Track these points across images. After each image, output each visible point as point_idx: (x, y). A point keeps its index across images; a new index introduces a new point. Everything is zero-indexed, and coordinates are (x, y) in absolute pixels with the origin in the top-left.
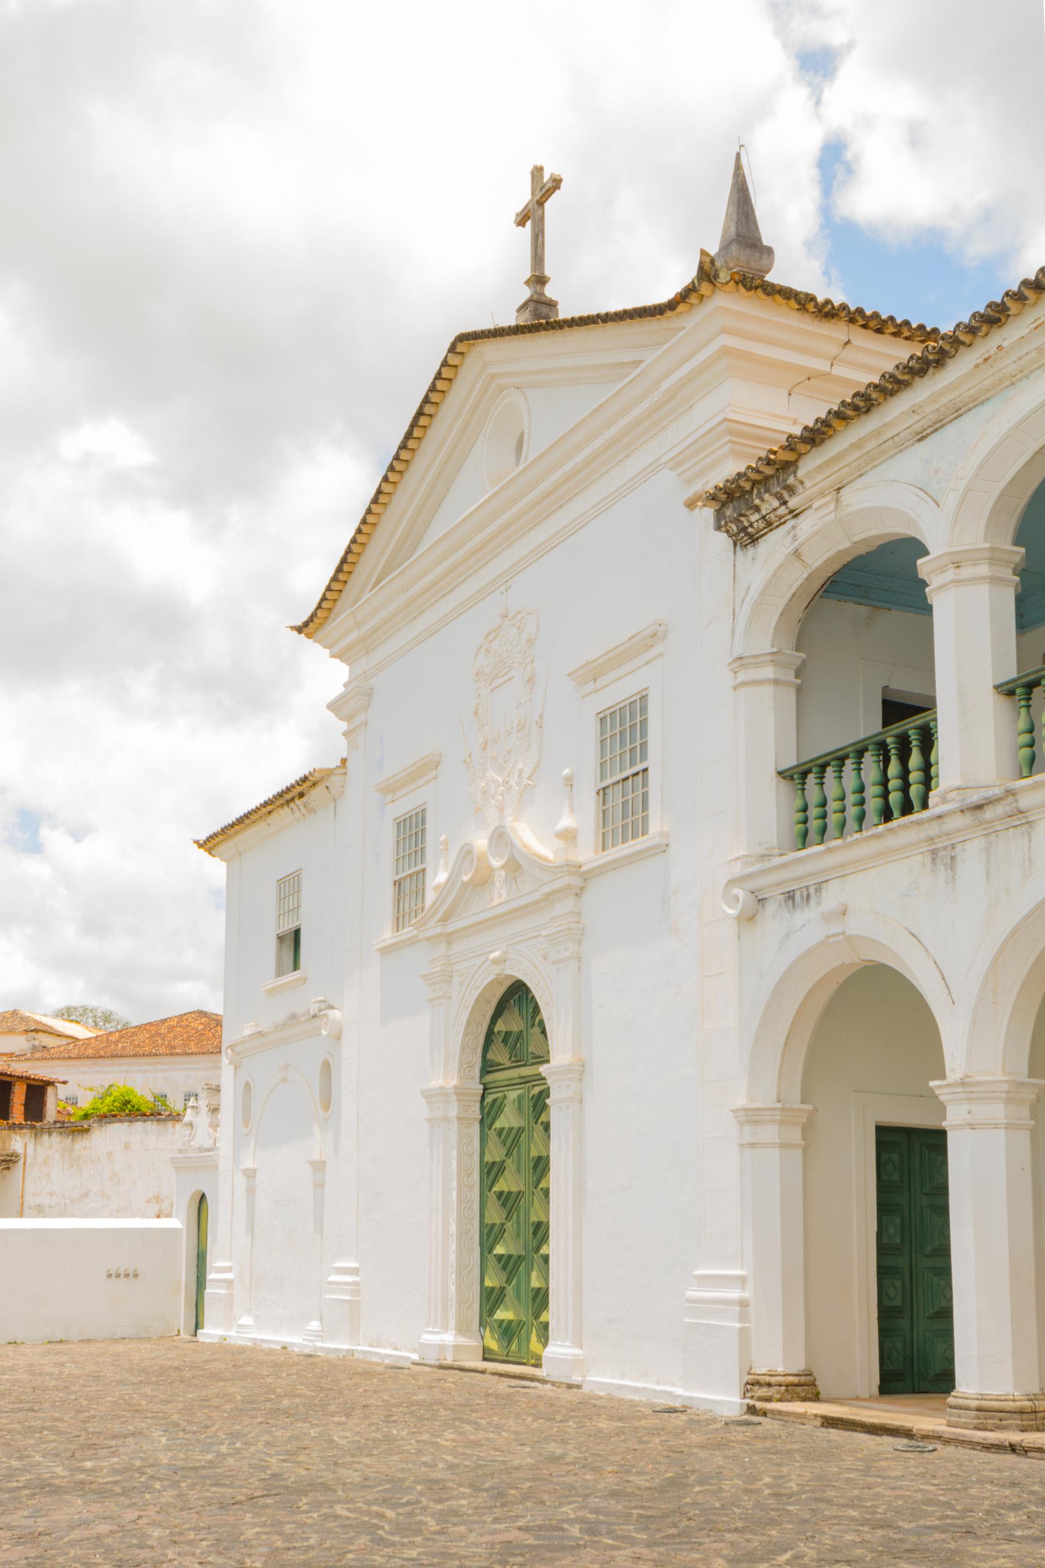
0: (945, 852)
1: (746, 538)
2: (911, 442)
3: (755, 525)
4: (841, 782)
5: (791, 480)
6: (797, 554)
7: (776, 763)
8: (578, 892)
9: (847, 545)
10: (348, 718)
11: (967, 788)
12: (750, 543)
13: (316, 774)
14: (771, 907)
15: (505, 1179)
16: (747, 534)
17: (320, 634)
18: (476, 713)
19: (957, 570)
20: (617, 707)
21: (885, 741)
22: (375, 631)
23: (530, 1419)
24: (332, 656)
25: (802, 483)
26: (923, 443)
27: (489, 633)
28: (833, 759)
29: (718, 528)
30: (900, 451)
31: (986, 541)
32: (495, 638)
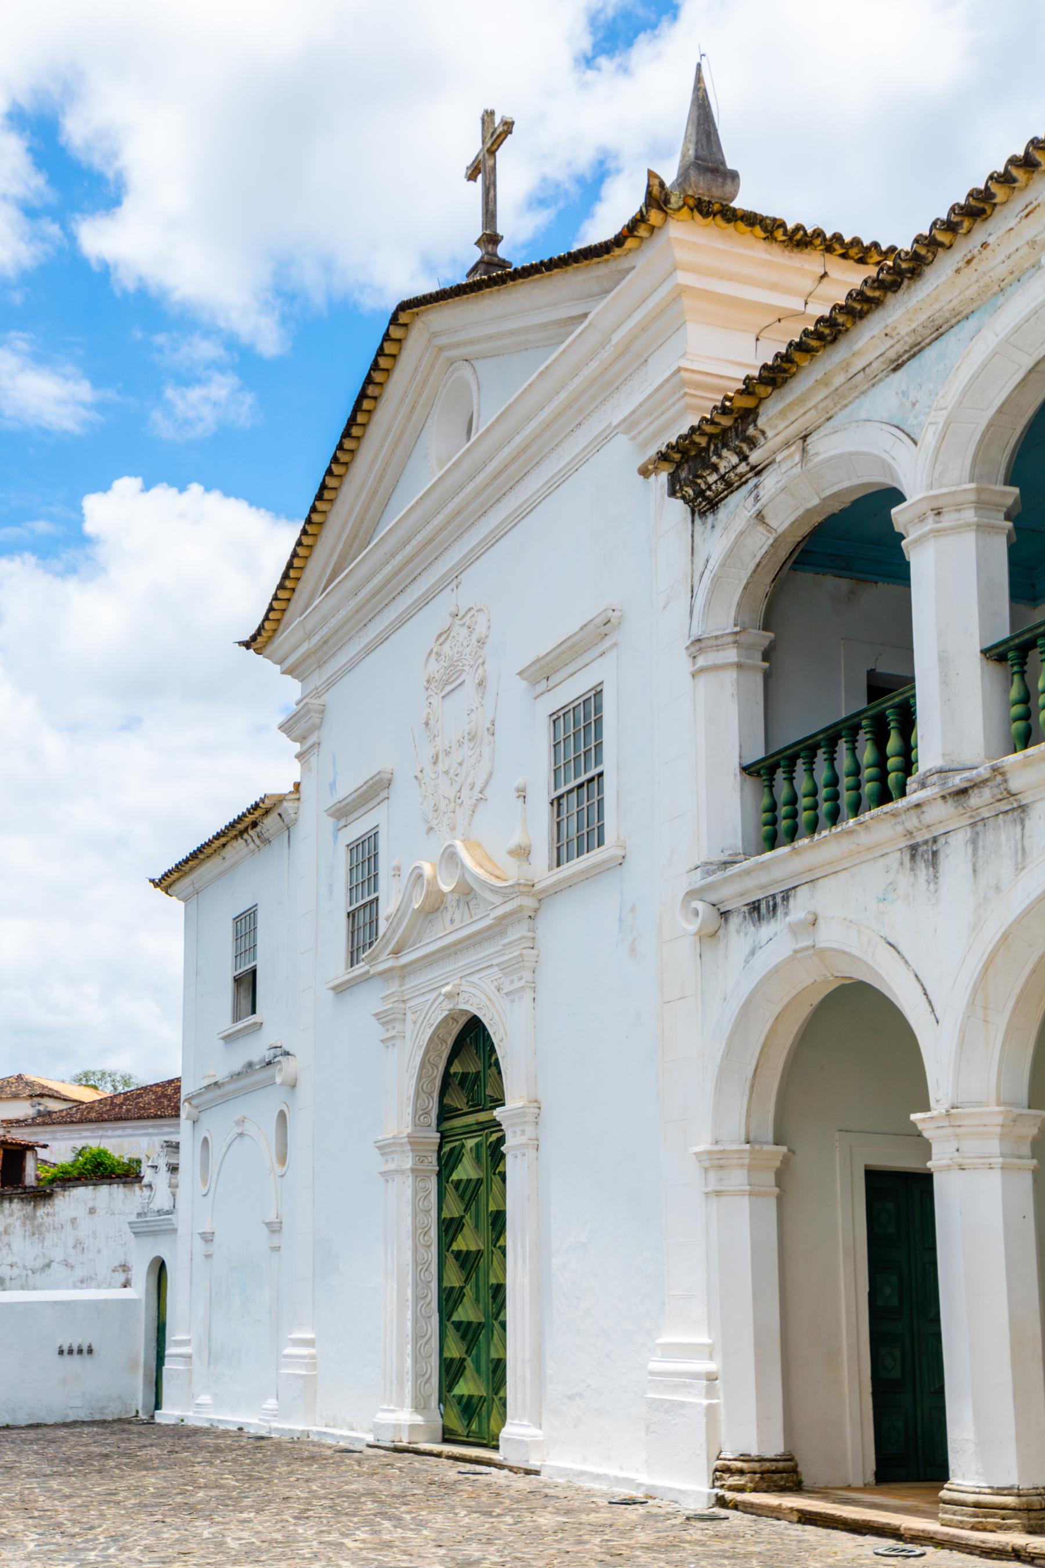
0: (925, 847)
1: (704, 503)
2: (885, 372)
3: (713, 487)
4: (812, 776)
5: (751, 431)
6: (760, 517)
7: (740, 757)
8: (532, 914)
9: (815, 501)
10: (301, 739)
11: (950, 771)
12: (708, 509)
13: (266, 801)
14: (735, 921)
15: (464, 1237)
16: (705, 498)
17: (269, 649)
18: (427, 724)
19: (937, 518)
20: (571, 707)
21: (861, 724)
22: (325, 642)
23: (463, 1513)
24: (283, 673)
25: (763, 433)
26: (899, 373)
27: (440, 635)
28: (802, 750)
29: (672, 493)
30: (873, 385)
31: (972, 481)
32: (447, 638)
